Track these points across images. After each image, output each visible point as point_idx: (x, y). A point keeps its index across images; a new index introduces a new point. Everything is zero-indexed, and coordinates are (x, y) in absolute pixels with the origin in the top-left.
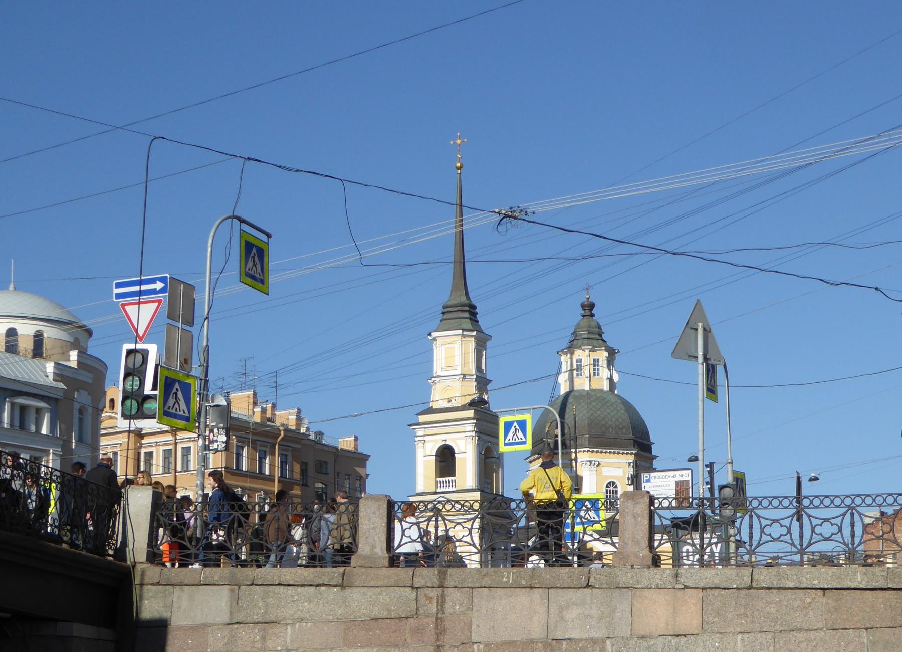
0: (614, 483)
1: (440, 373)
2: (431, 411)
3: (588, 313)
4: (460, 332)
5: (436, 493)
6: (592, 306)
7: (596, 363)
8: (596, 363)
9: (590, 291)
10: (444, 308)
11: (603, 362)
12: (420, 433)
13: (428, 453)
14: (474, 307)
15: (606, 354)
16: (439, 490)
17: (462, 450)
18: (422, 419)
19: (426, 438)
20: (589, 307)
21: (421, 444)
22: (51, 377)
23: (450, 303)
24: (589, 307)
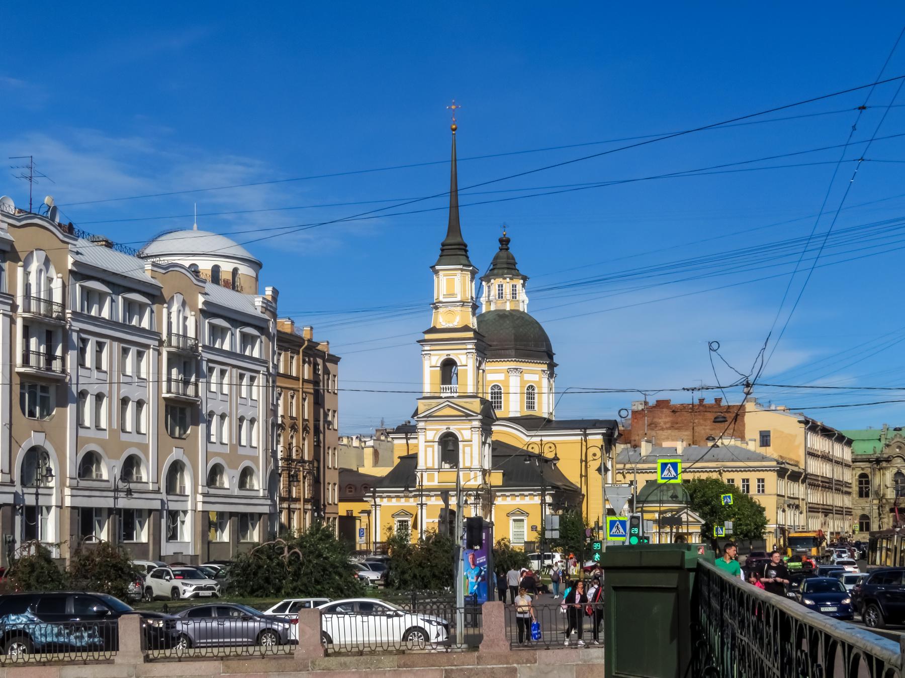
0: (532, 386)
1: (441, 299)
2: (433, 330)
3: (505, 247)
4: (461, 267)
5: (441, 398)
6: (508, 241)
7: (514, 286)
8: (514, 286)
9: (507, 229)
10: (443, 245)
11: (519, 287)
12: (427, 348)
13: (433, 364)
14: (466, 246)
15: (522, 281)
16: (443, 395)
17: (464, 363)
18: (427, 336)
20: (505, 242)
21: (427, 357)
22: (259, 309)
23: (449, 241)
24: (505, 242)
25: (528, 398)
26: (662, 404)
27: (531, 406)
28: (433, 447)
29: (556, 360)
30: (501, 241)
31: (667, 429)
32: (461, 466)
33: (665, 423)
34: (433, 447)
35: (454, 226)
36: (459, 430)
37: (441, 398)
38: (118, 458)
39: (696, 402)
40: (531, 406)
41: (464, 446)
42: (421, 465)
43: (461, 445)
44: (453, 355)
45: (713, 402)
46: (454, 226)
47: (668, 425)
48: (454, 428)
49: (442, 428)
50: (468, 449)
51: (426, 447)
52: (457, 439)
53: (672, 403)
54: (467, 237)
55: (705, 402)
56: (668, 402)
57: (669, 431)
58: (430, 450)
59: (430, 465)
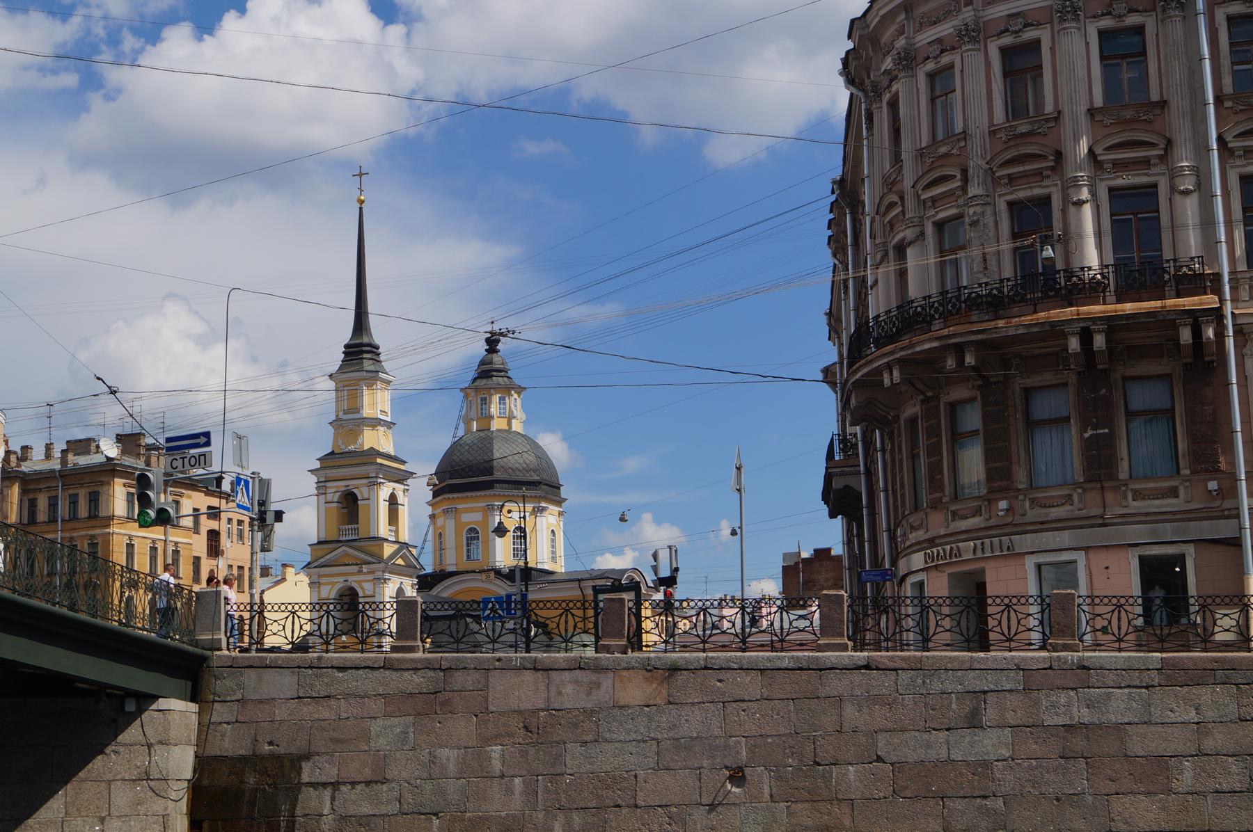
10: (346, 346)
13: (330, 497)
17: (366, 496)
19: (328, 484)
20: (492, 343)
29: (564, 492)
30: (488, 341)
33: (827, 580)
36: (358, 582)
48: (353, 581)
53: (833, 553)
54: (379, 331)
56: (829, 550)
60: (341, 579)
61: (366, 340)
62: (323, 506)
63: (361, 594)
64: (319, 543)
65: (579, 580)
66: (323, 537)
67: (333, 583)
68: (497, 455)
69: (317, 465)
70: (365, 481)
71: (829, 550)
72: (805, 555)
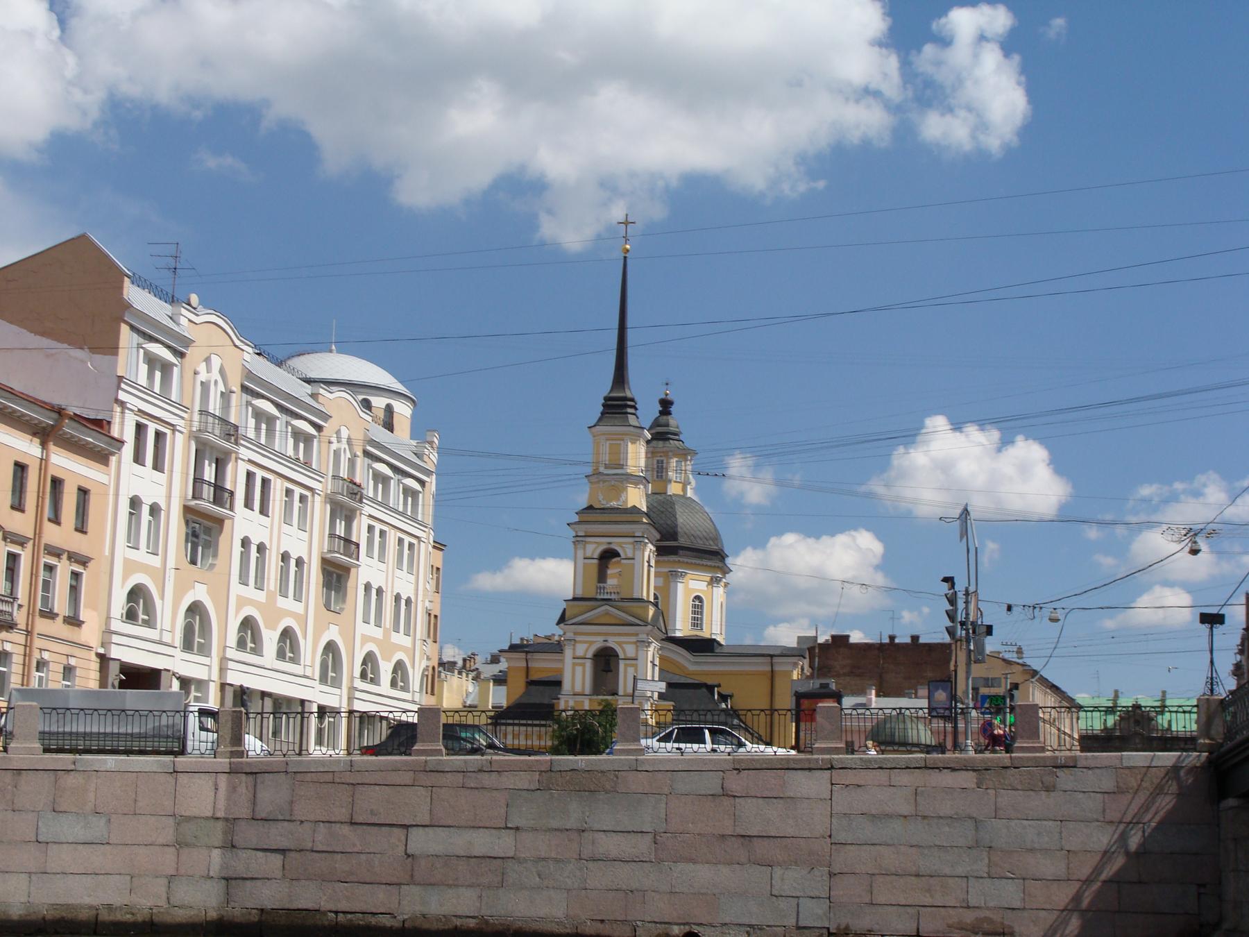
6: (670, 403)
10: (606, 399)
13: (588, 555)
16: (599, 597)
17: (630, 555)
25: (694, 612)
26: (840, 641)
27: (697, 622)
28: (583, 665)
31: (845, 675)
32: (621, 692)
34: (583, 665)
35: (620, 377)
36: (619, 644)
37: (596, 599)
38: (275, 629)
39: (886, 640)
40: (697, 622)
41: (626, 665)
42: (567, 686)
43: (622, 664)
44: (616, 544)
45: (908, 640)
46: (620, 377)
47: (846, 670)
48: (612, 643)
49: (598, 643)
50: (631, 671)
51: (574, 665)
52: (617, 656)
53: (852, 640)
55: (897, 641)
56: (847, 637)
57: (848, 679)
58: (579, 669)
59: (578, 689)
60: (600, 639)
61: (629, 394)
62: (581, 561)
63: (621, 655)
64: (575, 599)
65: (772, 656)
66: (580, 593)
67: (591, 643)
68: (680, 520)
69: (576, 518)
70: (631, 540)
71: (847, 637)
72: (821, 640)
